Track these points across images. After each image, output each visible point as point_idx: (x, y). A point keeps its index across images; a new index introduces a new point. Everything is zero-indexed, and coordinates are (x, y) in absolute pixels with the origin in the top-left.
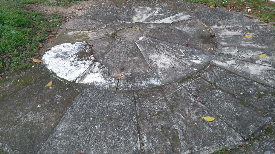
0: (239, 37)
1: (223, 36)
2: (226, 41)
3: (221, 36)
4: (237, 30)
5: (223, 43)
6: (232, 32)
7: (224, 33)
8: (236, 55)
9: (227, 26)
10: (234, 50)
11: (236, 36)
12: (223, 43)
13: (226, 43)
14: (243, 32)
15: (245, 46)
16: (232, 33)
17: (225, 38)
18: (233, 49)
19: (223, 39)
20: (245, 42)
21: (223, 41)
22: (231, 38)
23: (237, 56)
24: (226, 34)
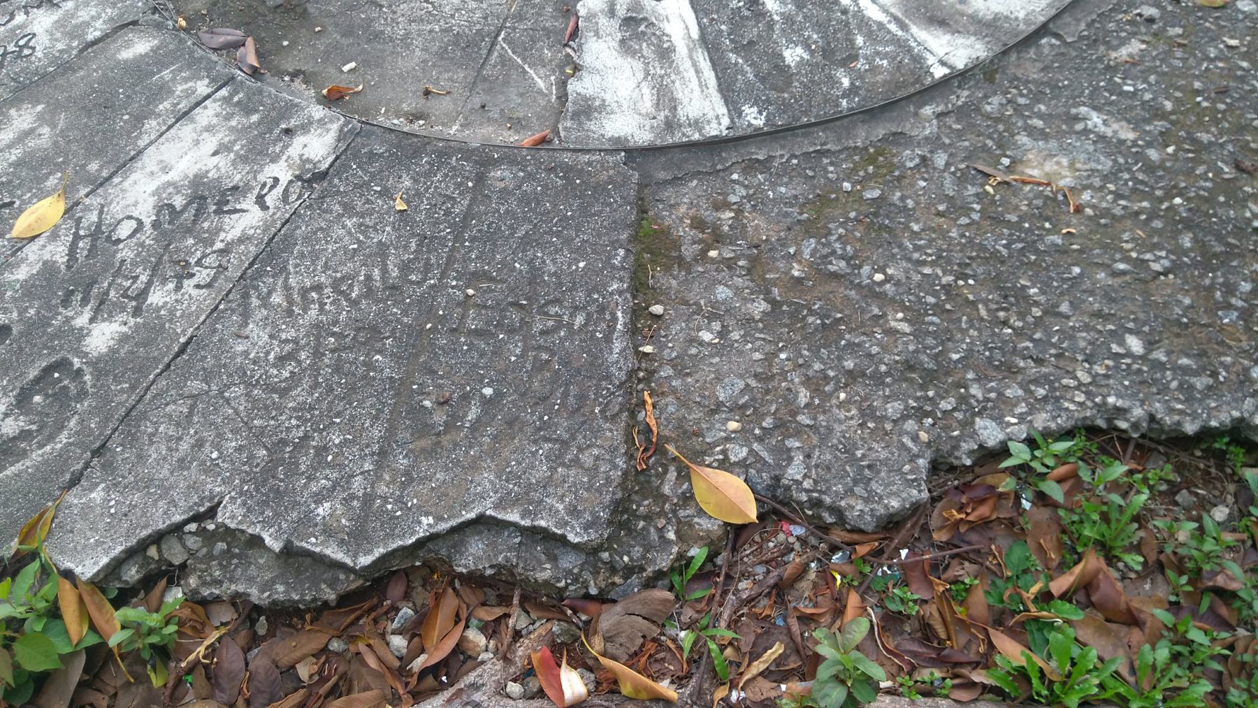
0: (93, 166)
1: (189, 93)
2: (140, 70)
3: (202, 87)
4: (156, 225)
5: (140, 46)
6: (173, 176)
7: (209, 129)
8: (20, 18)
9: (247, 220)
10: (54, 40)
11: (125, 164)
12: (140, 46)
13: (126, 55)
14: (102, 237)
15: (13, 112)
16: (166, 169)
17: (163, 90)
18: (60, 46)
19: (166, 74)
20: (32, 143)
21: (158, 60)
22: (139, 120)
23: (12, 16)
24: (186, 131)
